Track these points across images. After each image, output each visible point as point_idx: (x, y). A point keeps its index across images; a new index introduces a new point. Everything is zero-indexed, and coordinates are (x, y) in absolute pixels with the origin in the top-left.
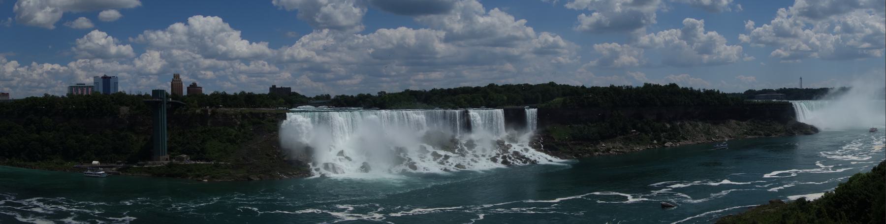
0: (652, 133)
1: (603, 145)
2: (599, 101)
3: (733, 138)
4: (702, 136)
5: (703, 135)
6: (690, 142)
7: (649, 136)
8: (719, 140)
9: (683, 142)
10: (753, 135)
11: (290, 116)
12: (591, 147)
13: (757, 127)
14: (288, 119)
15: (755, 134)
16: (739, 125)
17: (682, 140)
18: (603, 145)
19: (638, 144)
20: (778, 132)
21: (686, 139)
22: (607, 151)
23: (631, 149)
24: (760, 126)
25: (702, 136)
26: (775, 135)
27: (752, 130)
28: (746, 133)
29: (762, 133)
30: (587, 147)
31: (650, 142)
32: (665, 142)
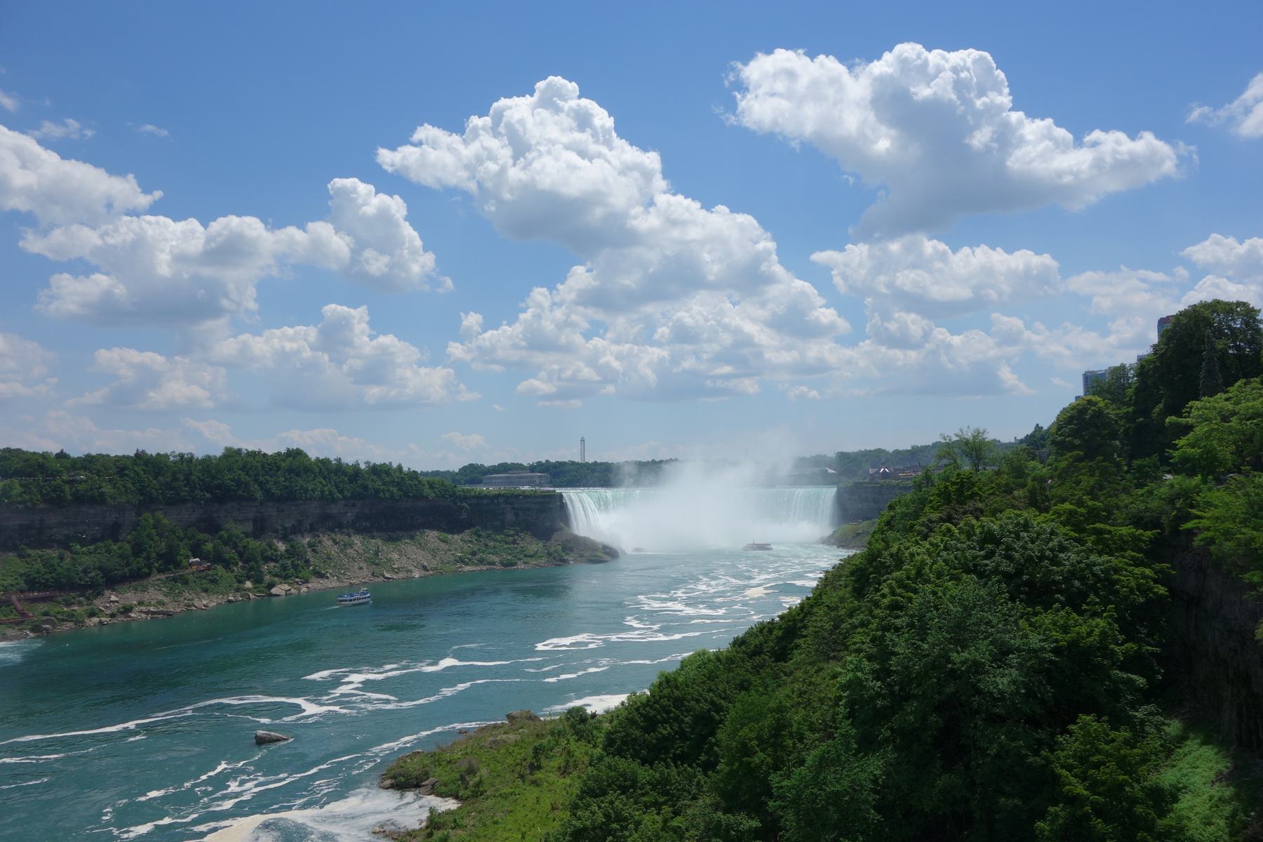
0: (240, 564)
1: (113, 598)
2: (103, 490)
3: (431, 572)
4: (361, 568)
5: (362, 565)
6: (331, 583)
7: (232, 572)
8: (401, 575)
9: (316, 584)
10: (476, 565)
12: (80, 603)
13: (486, 545)
15: (481, 561)
16: (445, 541)
17: (313, 579)
19: (206, 591)
20: (531, 556)
21: (320, 575)
22: (122, 613)
24: (491, 544)
25: (361, 568)
26: (525, 563)
27: (474, 554)
28: (461, 560)
29: (496, 559)
30: (68, 604)
31: (236, 585)
32: (272, 585)
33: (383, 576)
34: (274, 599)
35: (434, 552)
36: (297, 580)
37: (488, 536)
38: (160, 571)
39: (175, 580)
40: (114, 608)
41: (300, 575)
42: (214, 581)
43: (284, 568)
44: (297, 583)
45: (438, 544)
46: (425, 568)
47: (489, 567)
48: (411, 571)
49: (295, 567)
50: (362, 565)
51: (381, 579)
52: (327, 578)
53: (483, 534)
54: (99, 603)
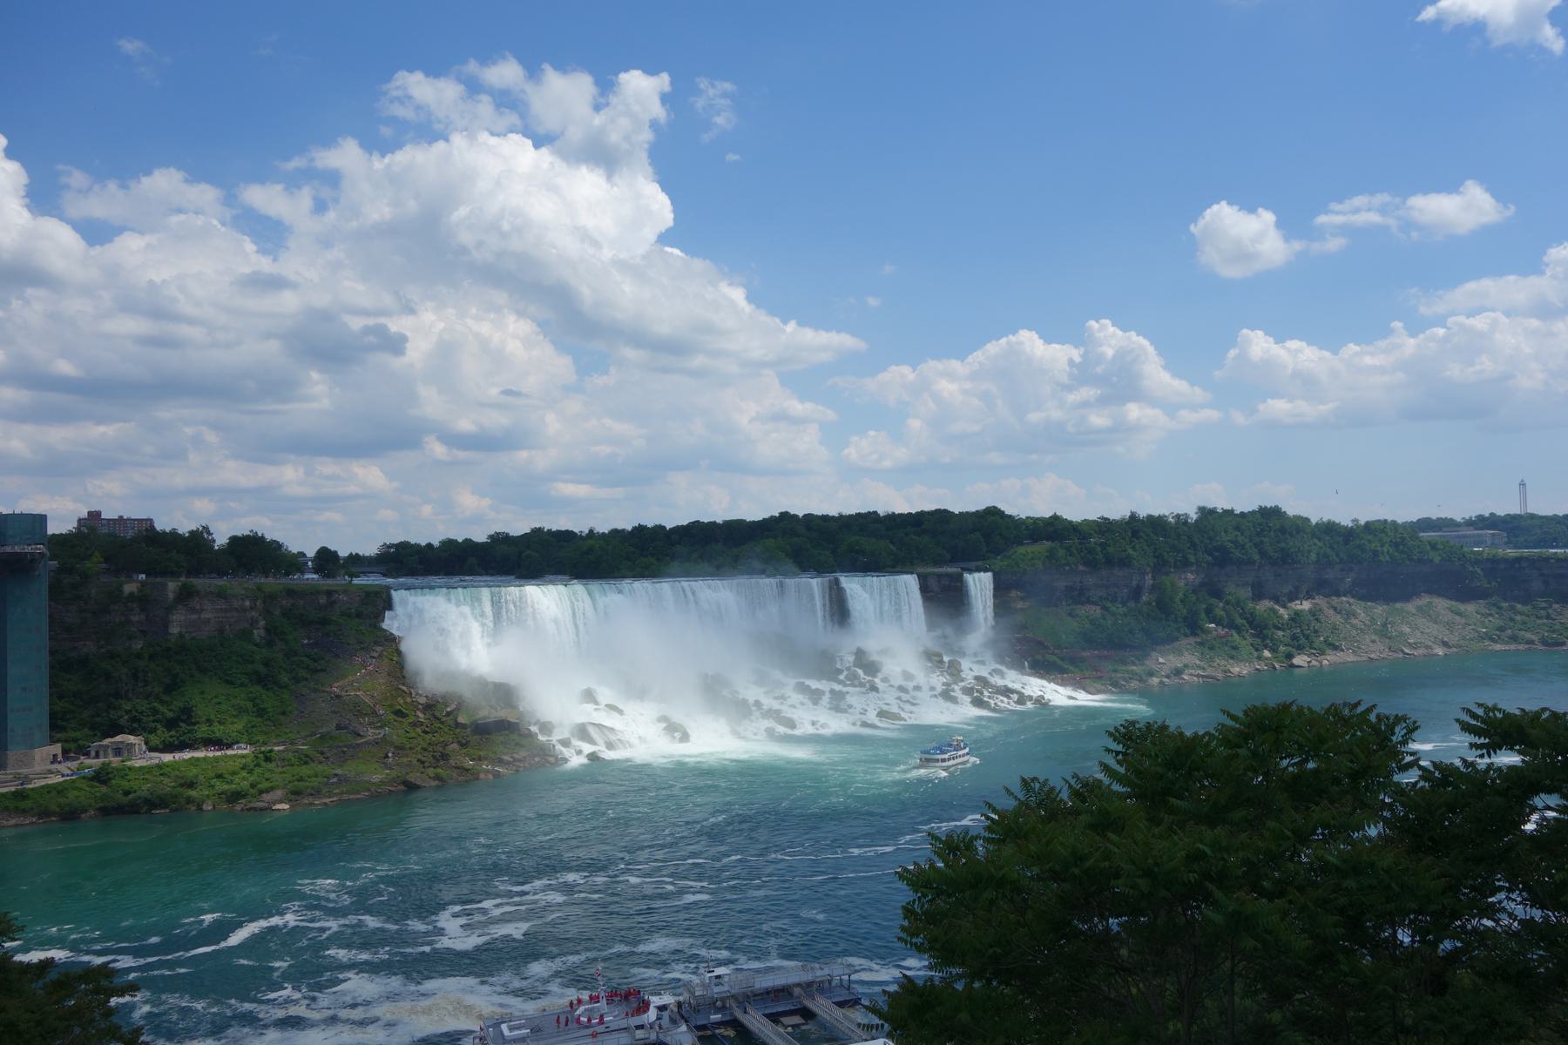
1: (1161, 660)
4: (1373, 641)
5: (1374, 637)
6: (1349, 657)
8: (1421, 651)
9: (1330, 659)
10: (1507, 643)
11: (404, 602)
13: (1512, 620)
14: (398, 608)
15: (1514, 639)
16: (1459, 614)
17: (1328, 651)
18: (1161, 660)
19: (1232, 658)
21: (1336, 648)
23: (1225, 672)
24: (1518, 618)
25: (1373, 641)
28: (1482, 638)
31: (1256, 654)
32: (1290, 656)
33: (1403, 651)
34: (1297, 671)
35: (1450, 626)
36: (1313, 651)
37: (1512, 608)
38: (1186, 636)
39: (1201, 644)
40: (1166, 670)
41: (1314, 646)
42: (1235, 648)
43: (1294, 638)
44: (1314, 654)
45: (1450, 616)
46: (1445, 644)
47: (1527, 646)
48: (1430, 647)
49: (1307, 637)
50: (1374, 637)
51: (1401, 655)
52: (1343, 650)
53: (1505, 605)
54: (1150, 664)
